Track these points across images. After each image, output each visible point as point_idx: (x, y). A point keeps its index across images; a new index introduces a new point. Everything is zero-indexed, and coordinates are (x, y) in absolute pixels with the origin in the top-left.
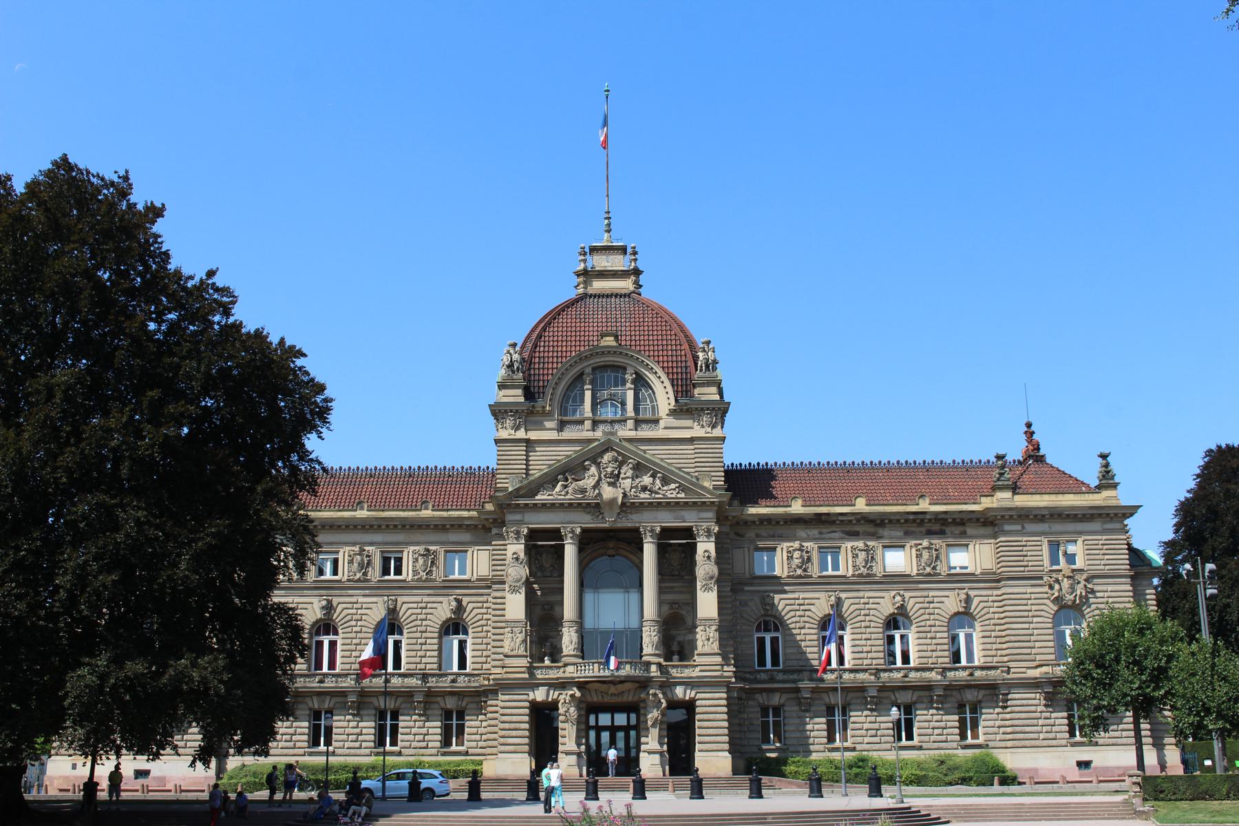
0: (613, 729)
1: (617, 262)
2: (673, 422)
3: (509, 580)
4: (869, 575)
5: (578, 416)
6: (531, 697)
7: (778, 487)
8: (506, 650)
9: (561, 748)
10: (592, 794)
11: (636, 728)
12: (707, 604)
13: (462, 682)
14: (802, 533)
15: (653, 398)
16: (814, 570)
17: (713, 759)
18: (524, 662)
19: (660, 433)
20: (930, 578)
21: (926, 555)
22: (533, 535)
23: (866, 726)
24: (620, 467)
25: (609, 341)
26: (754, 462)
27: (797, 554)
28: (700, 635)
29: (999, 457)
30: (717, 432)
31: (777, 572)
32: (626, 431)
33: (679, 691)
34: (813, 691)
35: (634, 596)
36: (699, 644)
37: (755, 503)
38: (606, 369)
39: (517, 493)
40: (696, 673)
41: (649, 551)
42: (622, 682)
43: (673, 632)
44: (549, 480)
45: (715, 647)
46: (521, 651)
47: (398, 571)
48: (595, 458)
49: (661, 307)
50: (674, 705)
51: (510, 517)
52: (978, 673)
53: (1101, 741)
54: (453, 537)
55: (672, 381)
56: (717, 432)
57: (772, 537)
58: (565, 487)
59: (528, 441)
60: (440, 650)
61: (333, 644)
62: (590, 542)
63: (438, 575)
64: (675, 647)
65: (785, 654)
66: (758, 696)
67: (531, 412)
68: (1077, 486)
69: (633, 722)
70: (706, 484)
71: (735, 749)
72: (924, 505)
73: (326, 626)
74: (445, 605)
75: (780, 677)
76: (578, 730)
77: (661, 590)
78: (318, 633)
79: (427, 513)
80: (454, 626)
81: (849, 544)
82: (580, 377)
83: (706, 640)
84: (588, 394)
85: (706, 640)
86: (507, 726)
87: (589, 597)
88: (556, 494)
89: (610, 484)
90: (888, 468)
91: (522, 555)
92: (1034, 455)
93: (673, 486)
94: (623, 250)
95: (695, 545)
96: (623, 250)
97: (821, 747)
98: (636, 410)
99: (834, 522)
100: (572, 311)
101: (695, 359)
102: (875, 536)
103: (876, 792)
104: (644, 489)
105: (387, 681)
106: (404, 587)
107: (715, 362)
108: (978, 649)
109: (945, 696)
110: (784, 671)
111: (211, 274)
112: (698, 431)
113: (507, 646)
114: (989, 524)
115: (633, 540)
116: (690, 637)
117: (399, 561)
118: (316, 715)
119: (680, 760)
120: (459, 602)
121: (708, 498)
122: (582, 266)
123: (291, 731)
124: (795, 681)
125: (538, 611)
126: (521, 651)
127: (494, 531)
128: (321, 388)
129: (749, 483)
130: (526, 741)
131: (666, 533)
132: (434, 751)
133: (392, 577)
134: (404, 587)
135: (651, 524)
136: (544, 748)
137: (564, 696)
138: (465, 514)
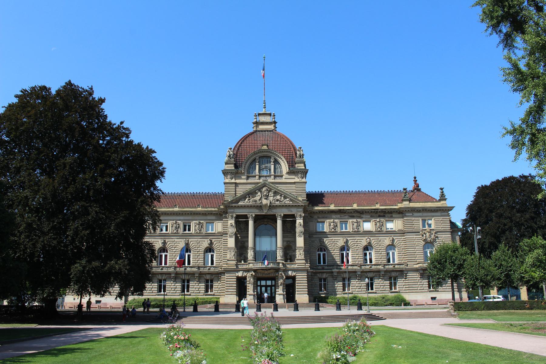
0: (266, 286)
2: (288, 176)
3: (229, 233)
4: (358, 231)
5: (254, 174)
6: (237, 275)
7: (325, 200)
8: (228, 258)
9: (248, 293)
10: (259, 309)
11: (275, 286)
12: (300, 241)
13: (212, 269)
14: (334, 216)
15: (281, 168)
16: (338, 230)
17: (302, 297)
18: (234, 262)
19: (283, 180)
20: (380, 232)
21: (378, 224)
22: (238, 217)
23: (356, 285)
24: (269, 193)
25: (265, 147)
26: (317, 191)
27: (332, 224)
28: (297, 253)
29: (405, 189)
30: (304, 180)
31: (325, 230)
32: (271, 180)
33: (290, 273)
34: (338, 272)
35: (274, 239)
36: (297, 256)
37: (317, 205)
38: (264, 158)
39: (232, 202)
40: (296, 266)
41: (279, 223)
42: (269, 270)
43: (288, 252)
44: (243, 197)
45: (303, 257)
46: (233, 259)
47: (189, 230)
48: (260, 189)
49: (284, 135)
50: (288, 278)
51: (229, 211)
52: (396, 266)
53: (440, 290)
54: (209, 217)
55: (287, 162)
56: (304, 180)
57: (323, 218)
58: (249, 200)
59: (236, 183)
60: (204, 258)
61: (166, 256)
62: (258, 219)
63: (204, 231)
64: (288, 257)
65: (328, 260)
66: (318, 275)
67: (237, 173)
68: (432, 200)
69: (273, 284)
70: (300, 199)
71: (310, 293)
72: (378, 206)
73: (164, 249)
74: (206, 242)
75: (326, 267)
76: (254, 287)
77: (284, 237)
78: (160, 252)
79: (199, 209)
80: (210, 249)
81: (351, 220)
82: (254, 160)
83: (300, 255)
84: (257, 167)
85: (300, 255)
86: (228, 285)
87: (258, 239)
88: (246, 202)
89: (265, 199)
90: (365, 193)
91: (234, 224)
92: (417, 188)
93: (288, 199)
94: (270, 115)
95: (296, 221)
96: (270, 115)
97: (341, 293)
98: (275, 172)
99: (345, 212)
100: (252, 137)
101: (296, 154)
102: (360, 217)
103: (360, 308)
104: (278, 200)
105: (185, 269)
106: (191, 235)
107: (303, 155)
108: (397, 258)
109: (385, 274)
110: (327, 266)
111: (122, 123)
112: (297, 180)
113: (228, 256)
114: (401, 213)
115: (273, 219)
116: (294, 253)
117: (189, 226)
118: (160, 281)
119: (290, 297)
120: (211, 241)
121: (300, 204)
122: (255, 120)
123: (151, 287)
124: (331, 269)
125: (239, 244)
126: (233, 259)
127: (224, 215)
128: (161, 164)
129: (315, 198)
130: (235, 290)
131: (285, 216)
132: (202, 294)
133: (187, 232)
134: (191, 235)
135: (280, 213)
136: (241, 293)
137: (249, 275)
138: (213, 209)
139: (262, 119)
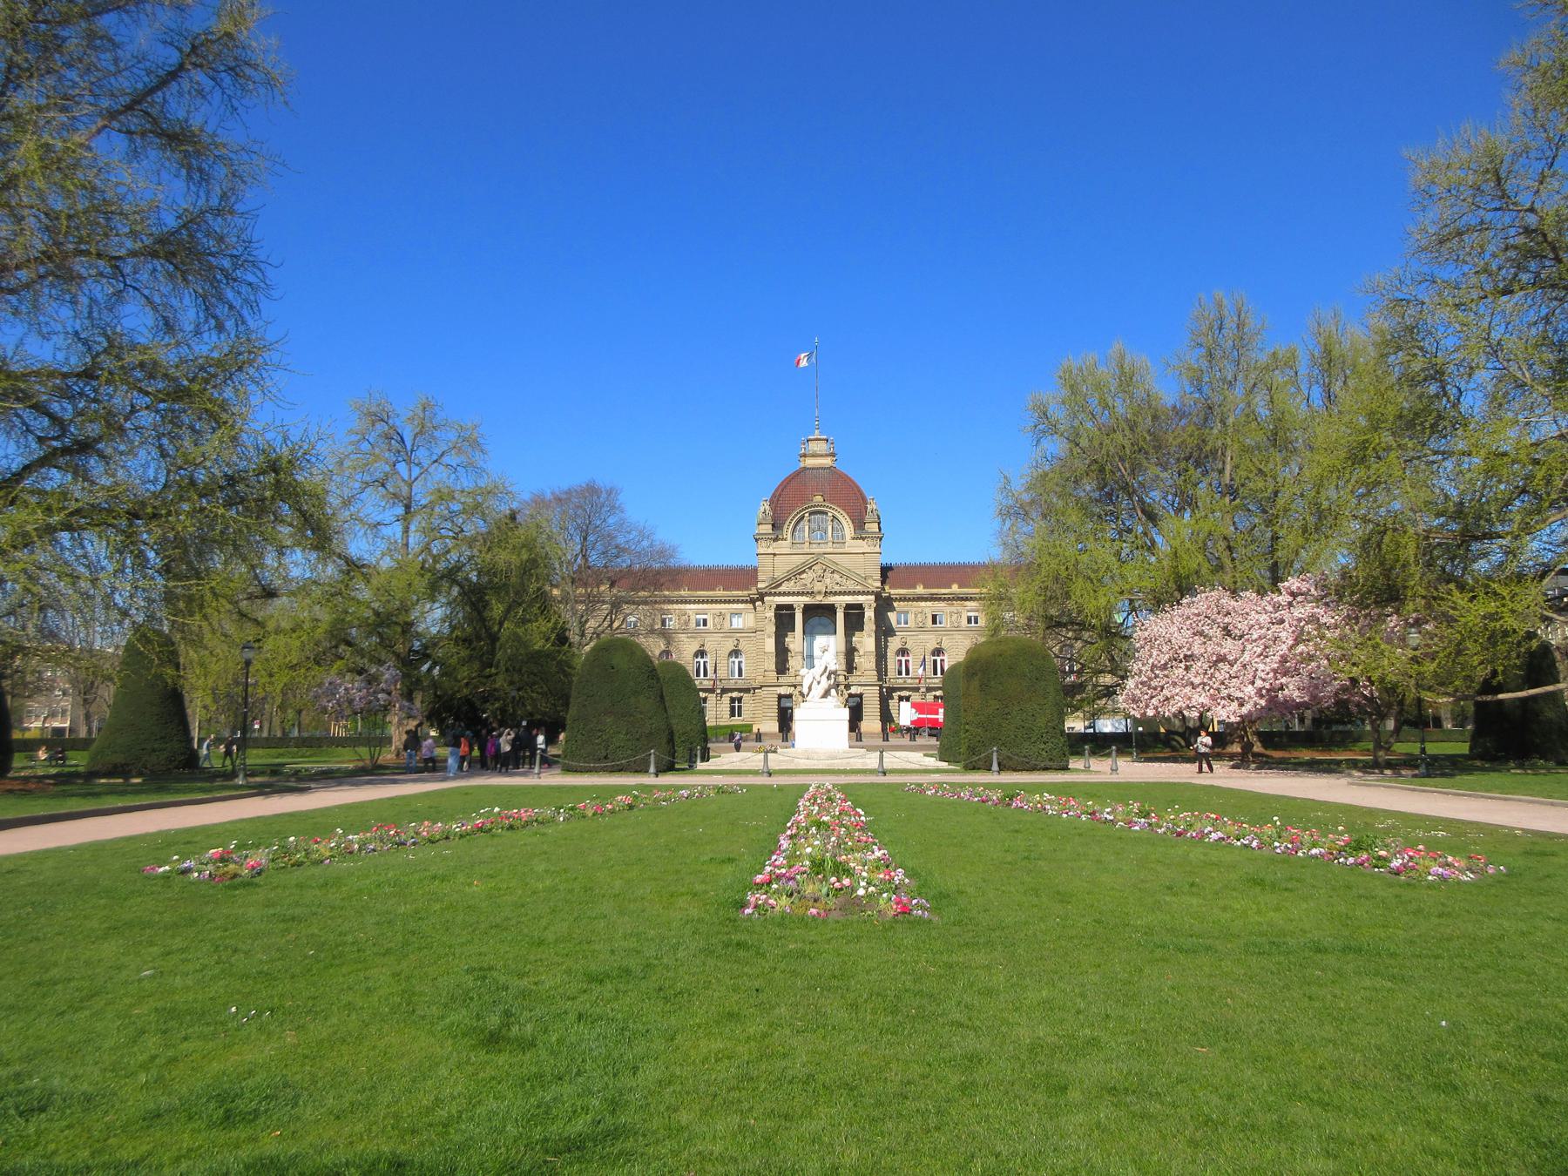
1: (820, 447)
14: (923, 604)
30: (877, 549)
54: (735, 606)
67: (776, 540)
80: (736, 653)
131: (849, 607)
135: (840, 601)
139: (814, 447)
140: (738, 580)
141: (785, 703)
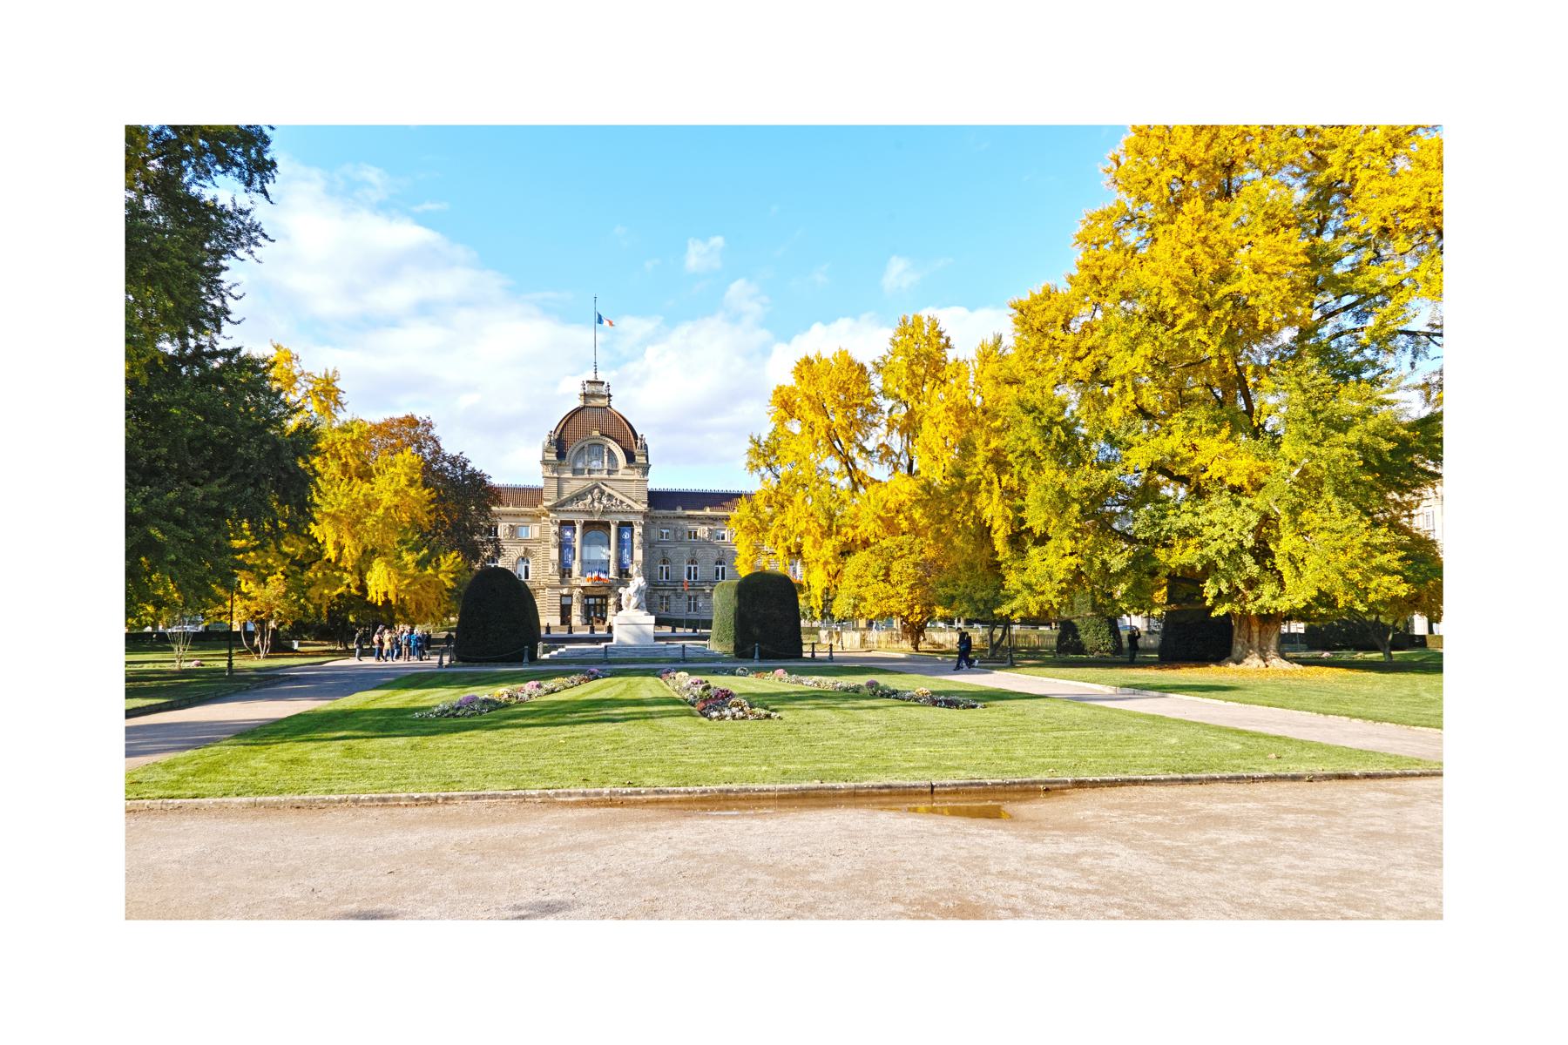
19: (619, 476)
32: (604, 475)
39: (555, 506)
79: (511, 508)
115: (607, 525)
135: (614, 520)
140: (530, 496)
141: (566, 601)
